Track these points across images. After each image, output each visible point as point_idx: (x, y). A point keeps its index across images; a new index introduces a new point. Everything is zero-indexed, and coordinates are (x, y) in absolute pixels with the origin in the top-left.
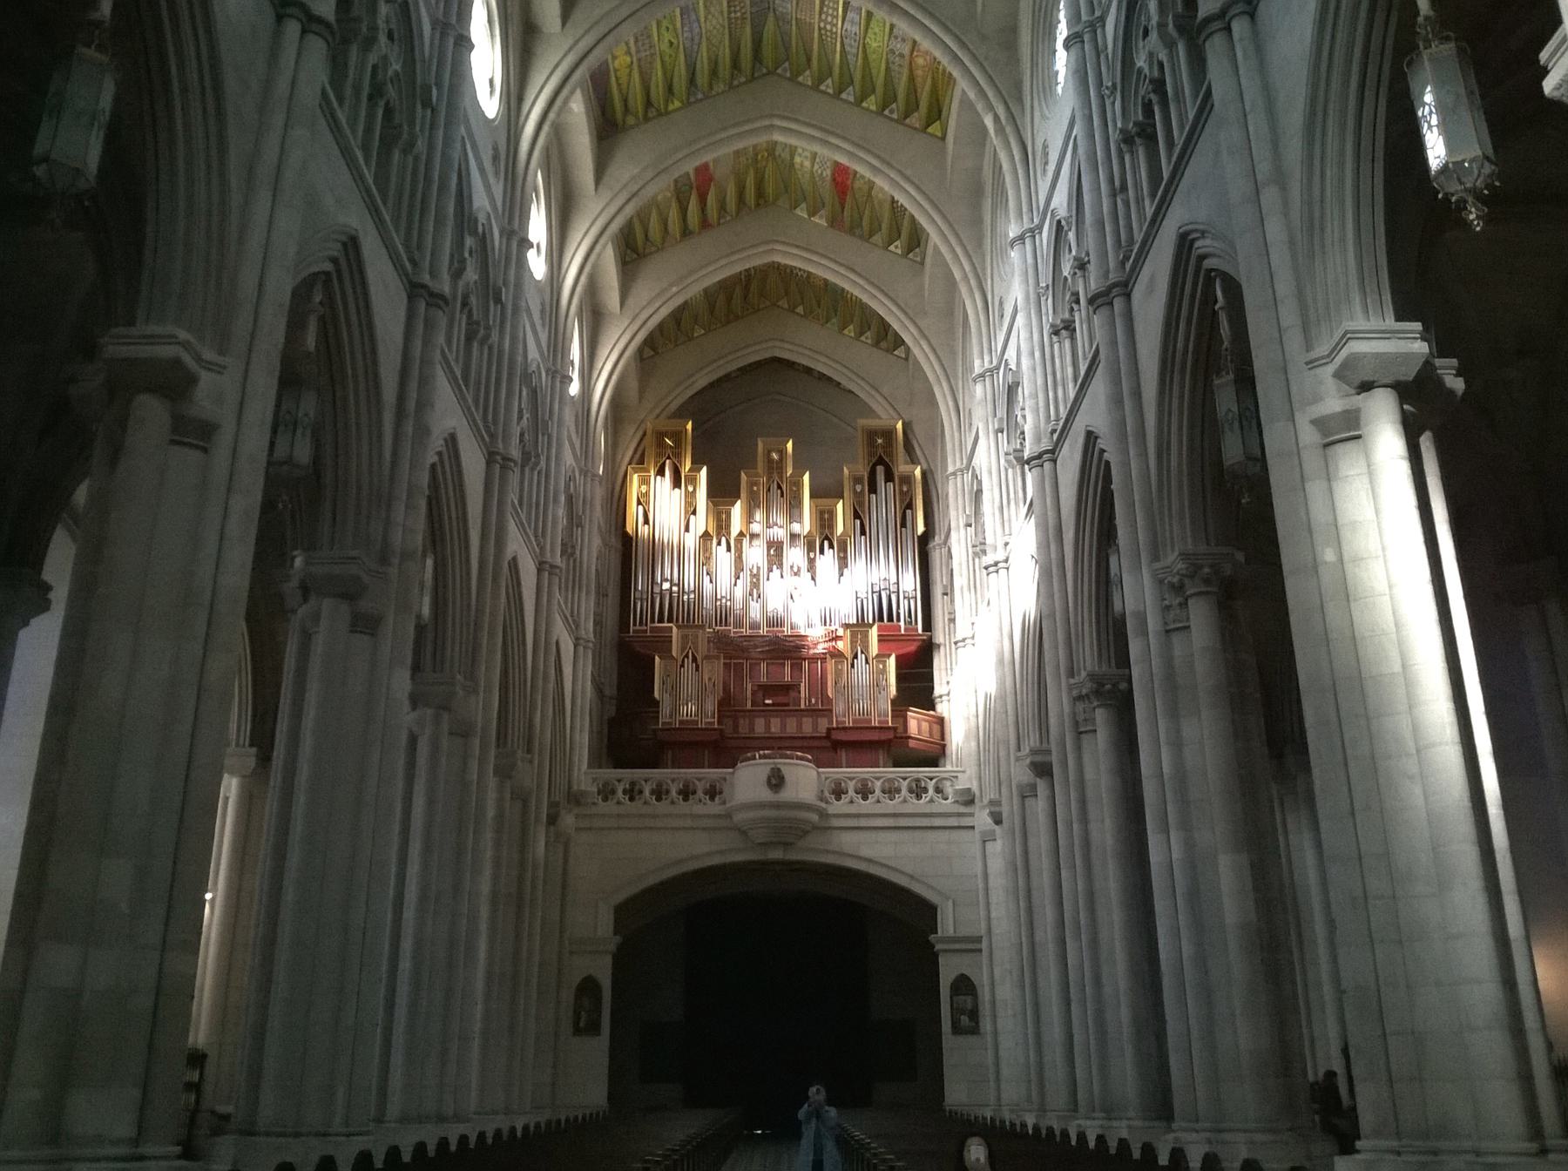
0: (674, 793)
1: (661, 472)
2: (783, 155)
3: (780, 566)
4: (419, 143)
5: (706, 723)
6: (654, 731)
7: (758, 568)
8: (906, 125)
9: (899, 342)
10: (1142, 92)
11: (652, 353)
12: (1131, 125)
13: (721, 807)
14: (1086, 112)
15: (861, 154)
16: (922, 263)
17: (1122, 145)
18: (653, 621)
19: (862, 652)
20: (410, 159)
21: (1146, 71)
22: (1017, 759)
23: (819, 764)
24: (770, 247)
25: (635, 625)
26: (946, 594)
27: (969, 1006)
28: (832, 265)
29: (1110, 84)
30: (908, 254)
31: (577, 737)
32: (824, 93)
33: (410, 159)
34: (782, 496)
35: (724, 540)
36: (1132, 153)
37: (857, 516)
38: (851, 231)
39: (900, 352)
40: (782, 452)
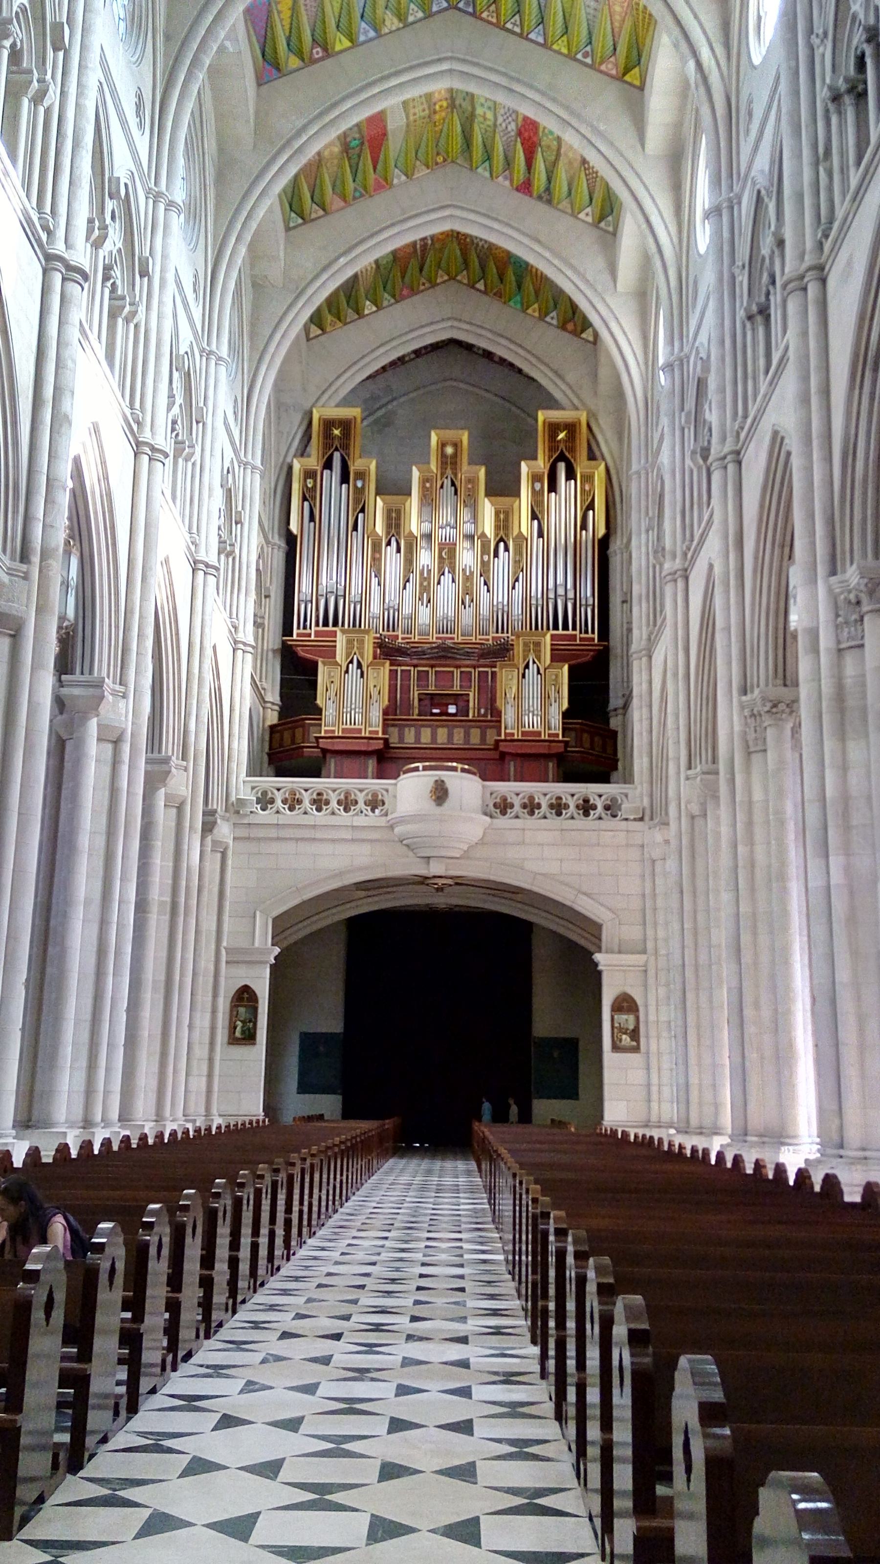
0: (334, 804)
1: (328, 465)
2: (464, 104)
3: (452, 571)
4: (51, 90)
5: (370, 732)
6: (317, 738)
7: (429, 571)
8: (601, 72)
9: (586, 324)
10: (855, 42)
11: (320, 332)
12: (841, 80)
13: (384, 818)
14: (793, 63)
15: (549, 105)
16: (614, 234)
17: (831, 107)
18: (317, 625)
19: (534, 662)
20: (41, 110)
21: (861, 16)
22: (687, 779)
23: (484, 778)
24: (447, 212)
25: (298, 628)
26: (624, 602)
27: (631, 1027)
28: (515, 235)
29: (821, 31)
30: (600, 222)
31: (235, 745)
32: (508, 30)
33: (41, 110)
34: (456, 493)
35: (393, 539)
36: (839, 113)
37: (534, 516)
38: (540, 198)
39: (588, 335)
40: (456, 445)
